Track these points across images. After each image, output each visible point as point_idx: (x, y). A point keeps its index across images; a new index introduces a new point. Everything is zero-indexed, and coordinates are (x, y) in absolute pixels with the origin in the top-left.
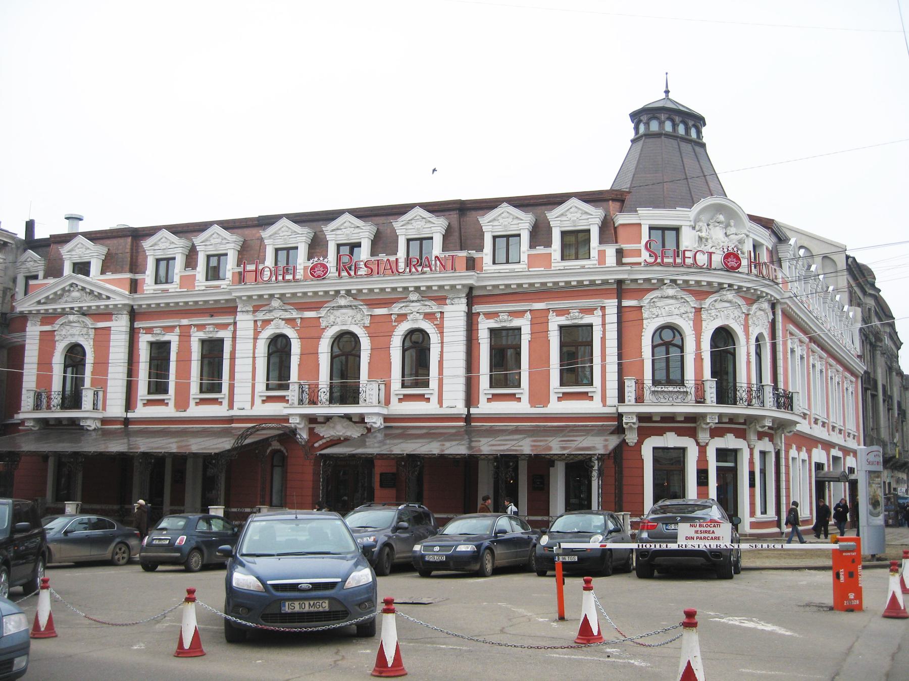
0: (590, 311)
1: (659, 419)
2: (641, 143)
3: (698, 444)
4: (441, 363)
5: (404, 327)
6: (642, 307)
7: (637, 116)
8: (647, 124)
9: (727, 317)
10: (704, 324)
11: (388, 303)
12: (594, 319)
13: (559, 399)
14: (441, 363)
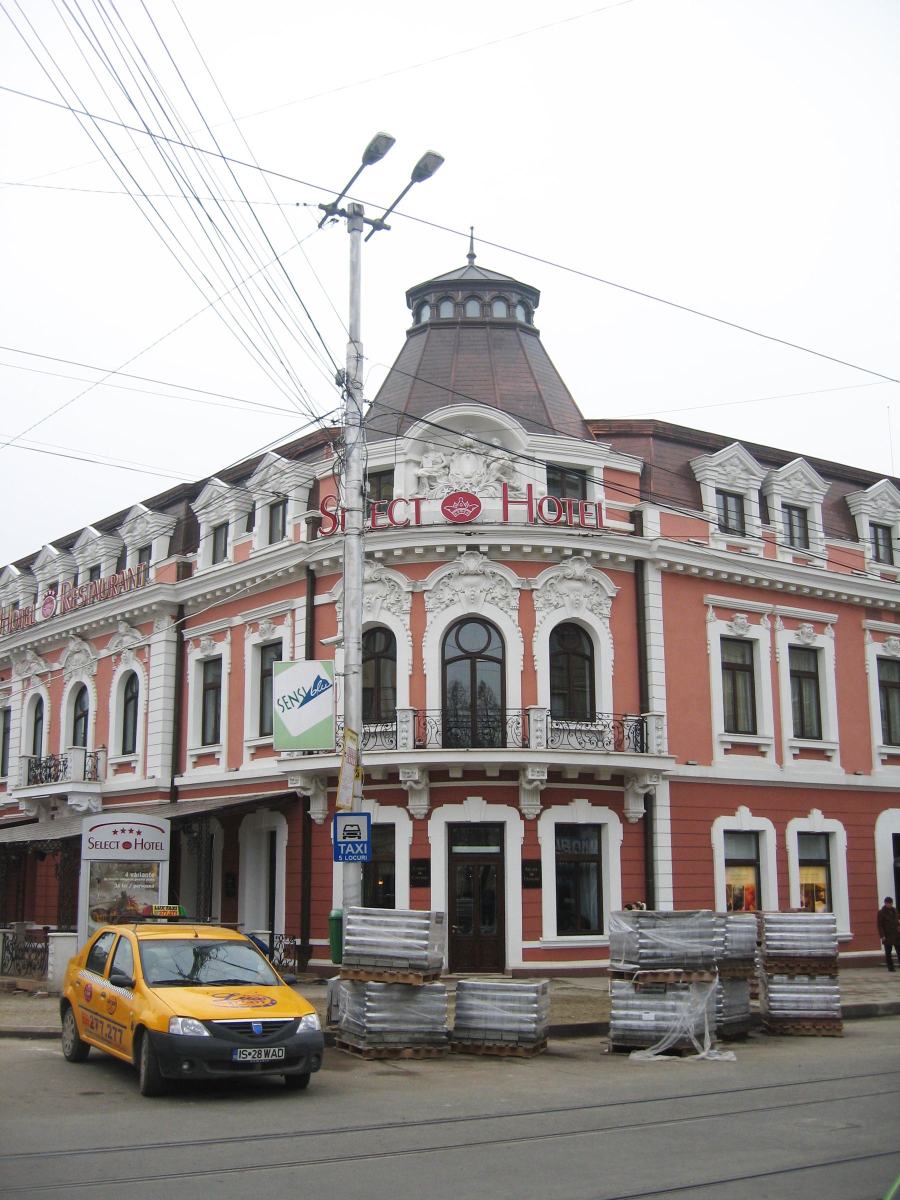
0: (278, 619)
1: (497, 774)
2: (423, 337)
3: (412, 817)
4: (147, 714)
5: (120, 670)
6: (335, 602)
7: (417, 297)
8: (436, 308)
9: (473, 600)
10: (430, 617)
11: (102, 642)
12: (282, 632)
13: (254, 756)
14: (147, 714)
